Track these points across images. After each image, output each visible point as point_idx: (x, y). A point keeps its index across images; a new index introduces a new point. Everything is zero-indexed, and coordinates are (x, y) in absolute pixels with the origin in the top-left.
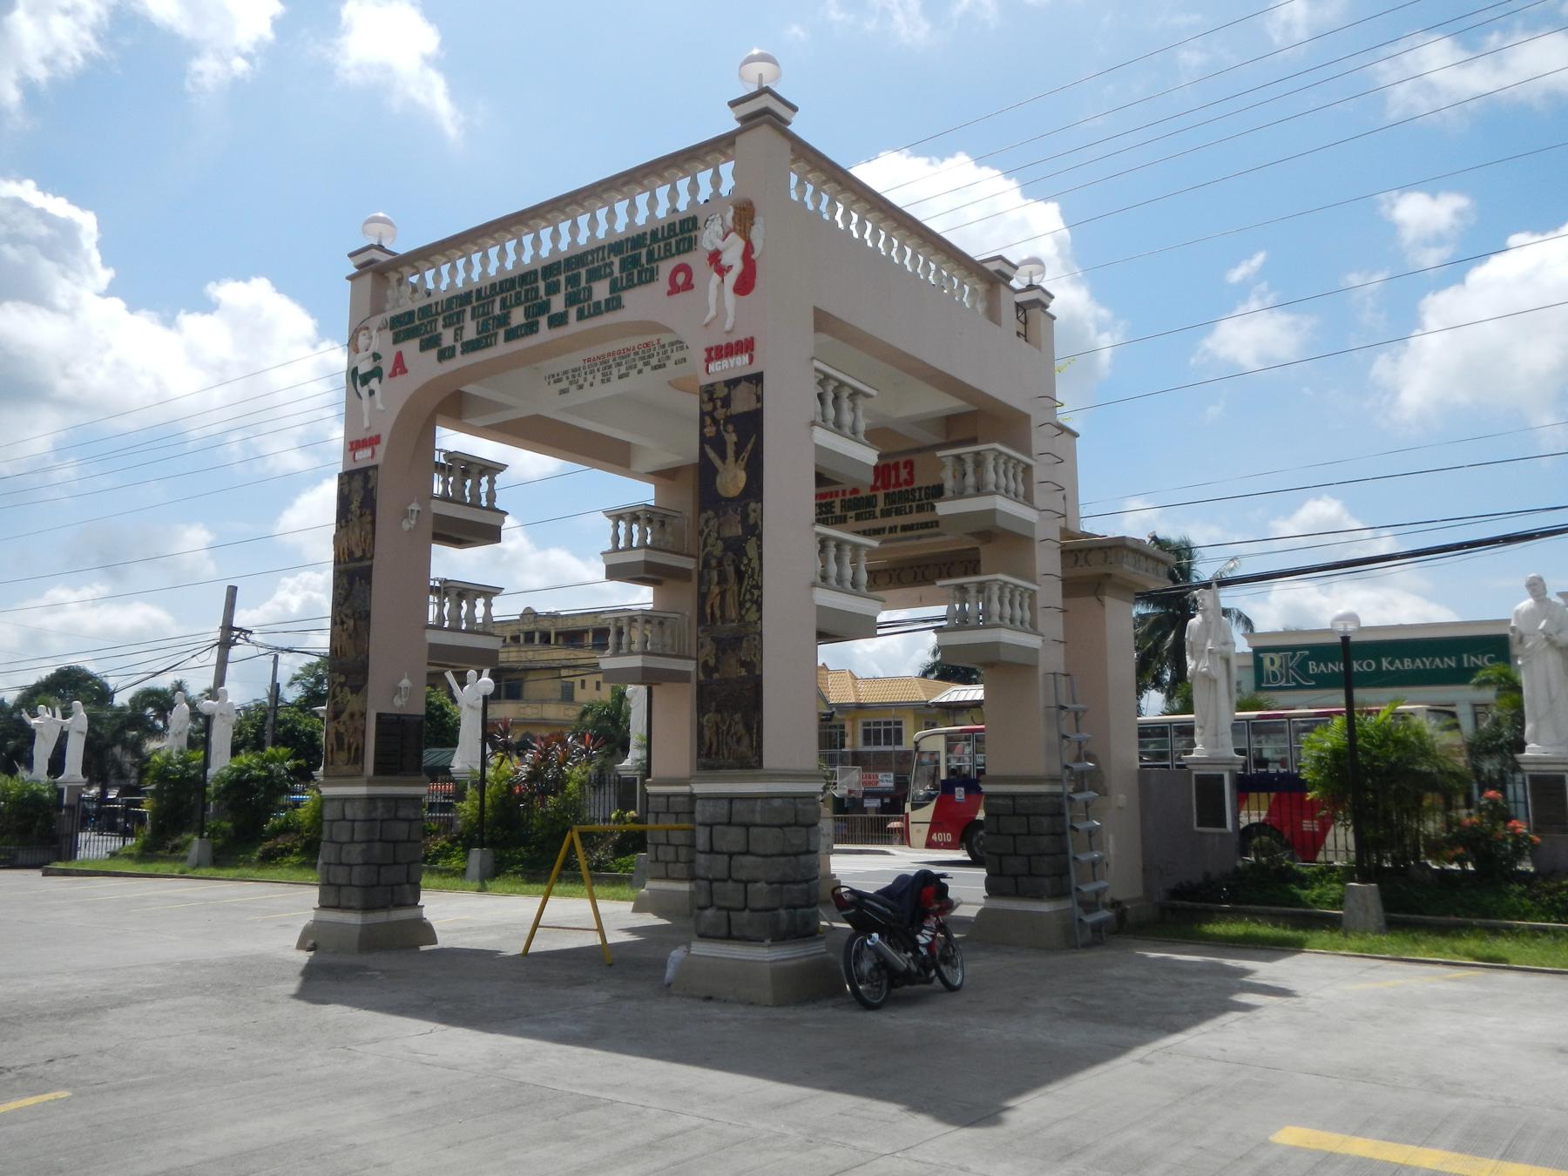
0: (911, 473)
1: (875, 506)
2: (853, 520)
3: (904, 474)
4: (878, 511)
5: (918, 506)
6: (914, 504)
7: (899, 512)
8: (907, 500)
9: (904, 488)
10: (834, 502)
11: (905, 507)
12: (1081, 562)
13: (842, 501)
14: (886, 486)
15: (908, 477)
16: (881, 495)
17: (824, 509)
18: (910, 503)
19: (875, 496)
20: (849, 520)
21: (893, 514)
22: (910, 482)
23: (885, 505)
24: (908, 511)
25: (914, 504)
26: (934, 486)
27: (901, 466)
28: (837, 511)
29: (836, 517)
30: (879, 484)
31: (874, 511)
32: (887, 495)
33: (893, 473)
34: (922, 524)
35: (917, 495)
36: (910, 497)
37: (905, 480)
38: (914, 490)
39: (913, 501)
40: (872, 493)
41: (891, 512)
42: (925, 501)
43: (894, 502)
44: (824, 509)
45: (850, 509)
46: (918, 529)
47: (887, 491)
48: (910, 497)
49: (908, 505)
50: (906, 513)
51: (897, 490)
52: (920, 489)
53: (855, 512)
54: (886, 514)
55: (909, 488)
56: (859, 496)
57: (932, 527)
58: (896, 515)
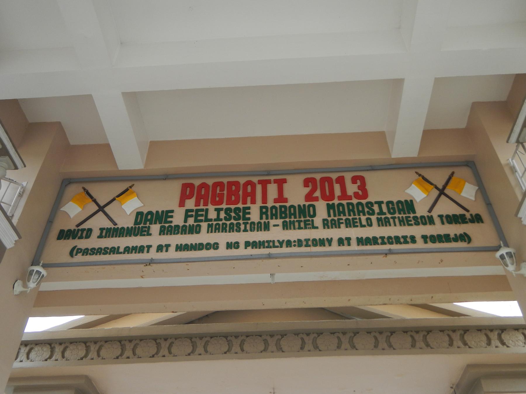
0: (363, 187)
1: (314, 215)
2: (281, 227)
3: (352, 189)
4: (318, 221)
5: (379, 220)
6: (374, 218)
7: (349, 224)
10: (249, 208)
11: (360, 219)
13: (261, 208)
15: (360, 192)
16: (321, 207)
17: (233, 214)
18: (367, 216)
19: (314, 206)
20: (272, 228)
21: (343, 226)
22: (365, 195)
23: (329, 216)
24: (364, 222)
25: (374, 218)
26: (399, 202)
28: (255, 216)
29: (253, 223)
30: (318, 194)
31: (313, 221)
32: (330, 207)
34: (390, 238)
35: (376, 208)
36: (366, 210)
37: (356, 195)
38: (370, 205)
39: (373, 213)
40: (307, 204)
41: (340, 223)
42: (389, 216)
44: (233, 214)
45: (274, 216)
46: (383, 243)
47: (331, 203)
48: (366, 210)
49: (363, 218)
50: (362, 226)
51: (344, 202)
52: (380, 203)
53: (282, 220)
54: (326, 224)
56: (288, 205)
57: (406, 242)
58: (347, 227)
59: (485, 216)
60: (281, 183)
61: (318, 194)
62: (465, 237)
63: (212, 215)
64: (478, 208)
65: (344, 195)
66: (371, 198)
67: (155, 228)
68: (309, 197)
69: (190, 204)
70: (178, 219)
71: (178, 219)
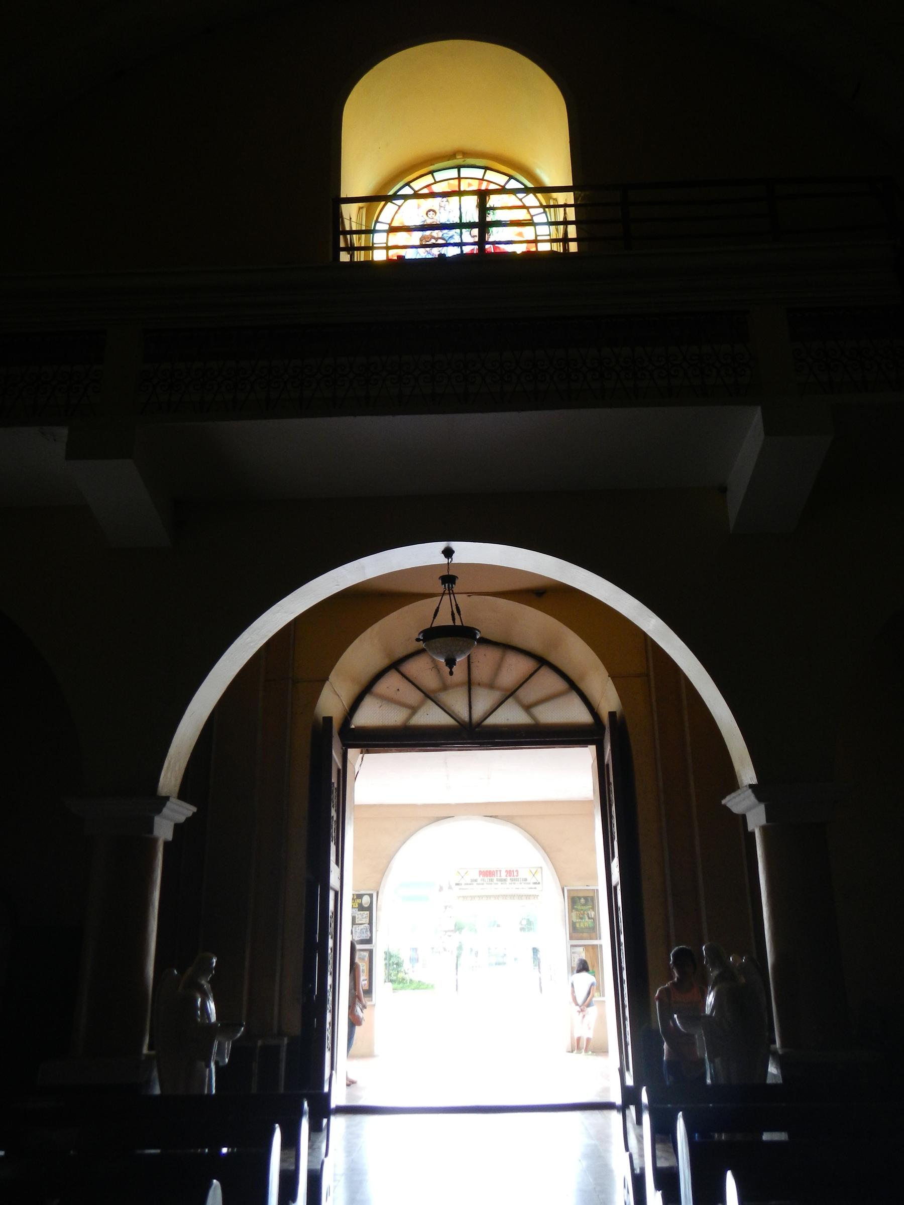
0: (517, 873)
3: (515, 874)
6: (519, 882)
8: (517, 881)
9: (515, 877)
12: (536, 898)
14: (510, 876)
22: (517, 876)
27: (515, 871)
28: (495, 881)
30: (508, 875)
32: (511, 879)
33: (512, 873)
38: (518, 879)
43: (512, 881)
51: (513, 878)
55: (517, 878)
59: (541, 883)
60: (500, 871)
61: (508, 875)
62: (535, 888)
63: (486, 881)
64: (540, 880)
65: (514, 876)
66: (519, 877)
67: (475, 883)
68: (506, 876)
69: (481, 876)
70: (479, 881)
71: (479, 881)
